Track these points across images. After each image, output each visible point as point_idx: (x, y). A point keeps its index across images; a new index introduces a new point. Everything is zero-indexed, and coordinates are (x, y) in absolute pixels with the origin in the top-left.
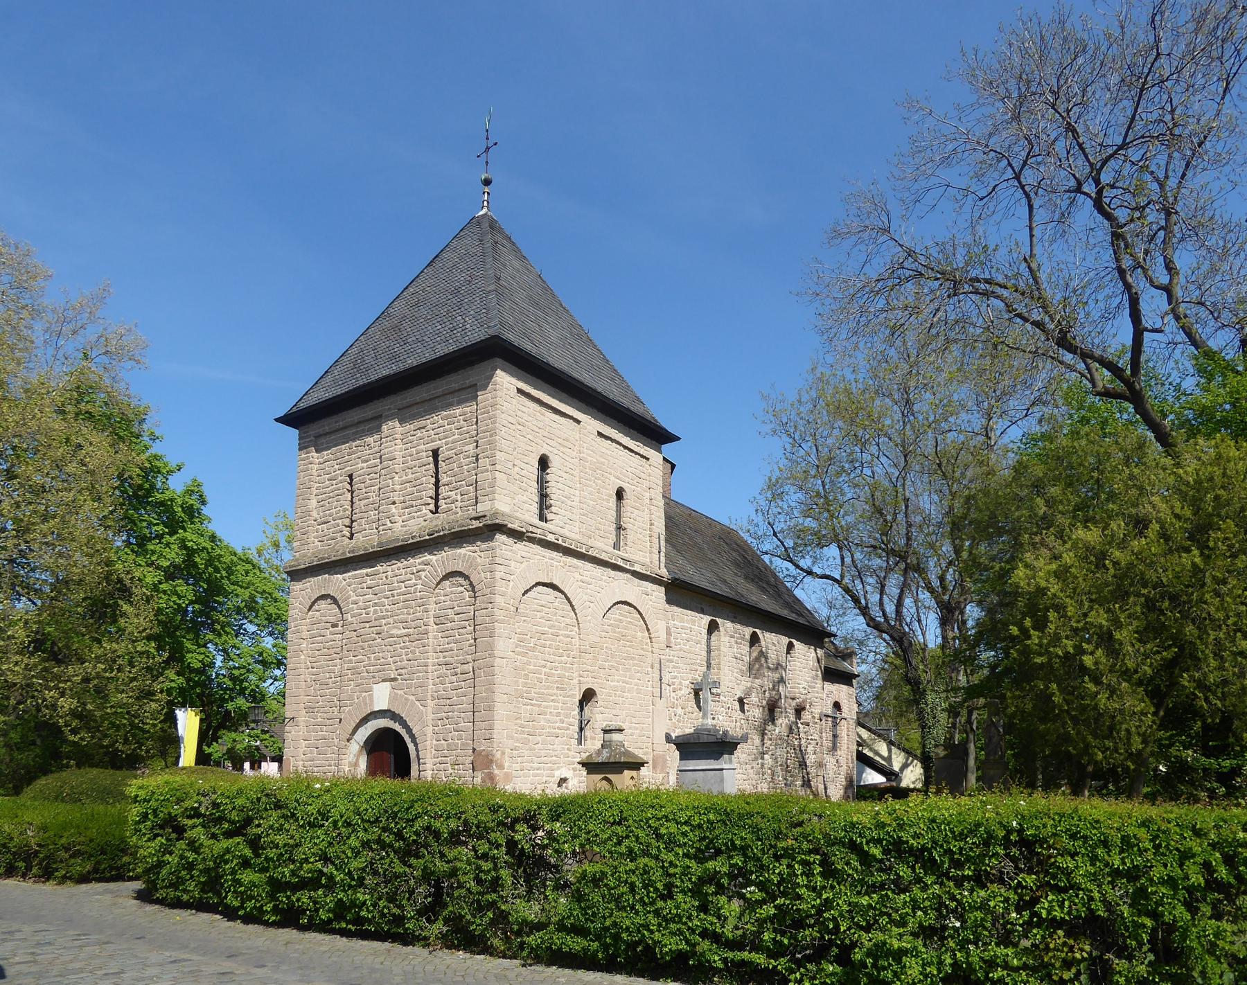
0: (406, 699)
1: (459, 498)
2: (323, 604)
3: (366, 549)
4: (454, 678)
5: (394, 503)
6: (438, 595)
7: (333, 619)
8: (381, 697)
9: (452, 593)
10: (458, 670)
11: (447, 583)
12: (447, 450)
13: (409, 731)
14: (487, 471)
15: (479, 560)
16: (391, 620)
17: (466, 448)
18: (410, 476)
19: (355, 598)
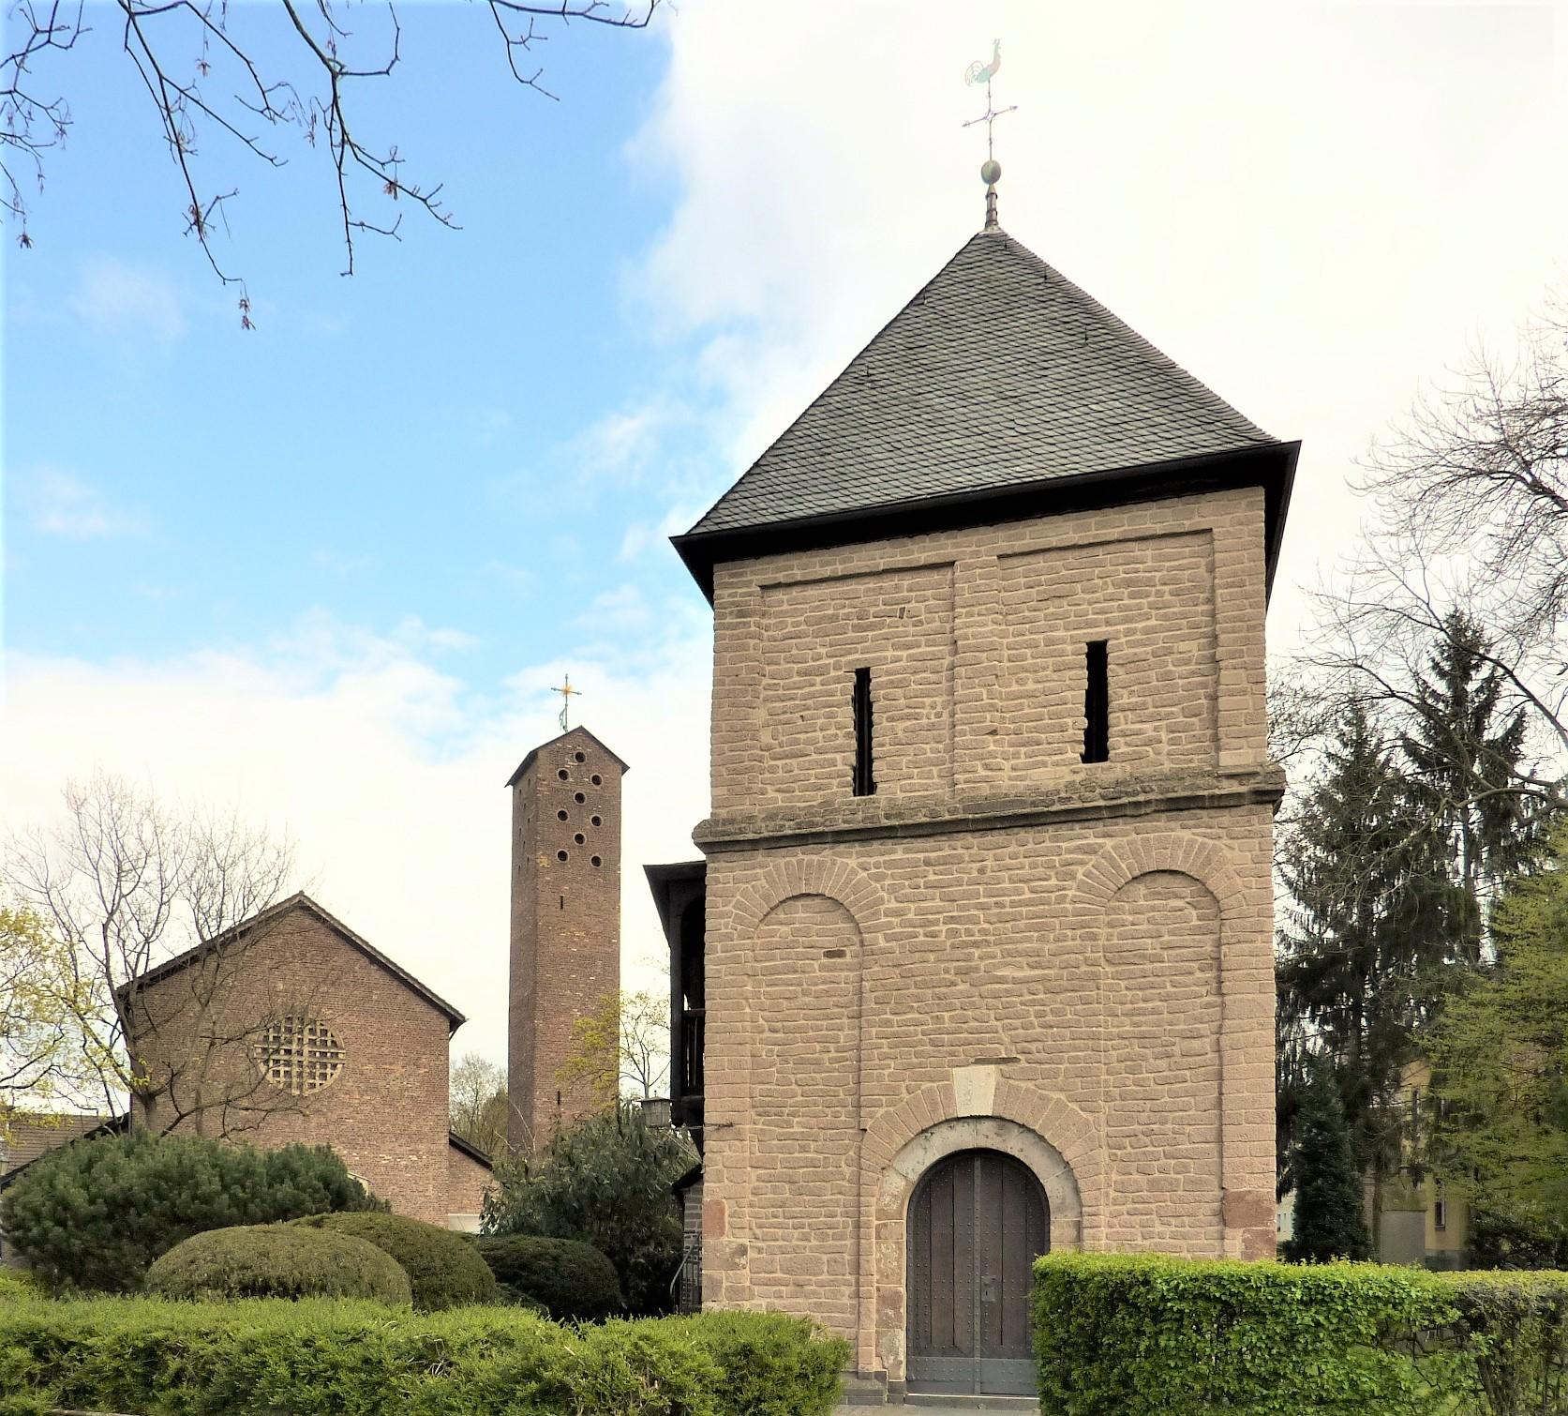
0: (1041, 1098)
1: (1164, 736)
2: (801, 912)
3: (933, 813)
4: (1163, 1063)
5: (994, 732)
6: (1115, 910)
7: (830, 943)
8: (976, 1090)
9: (1153, 909)
10: (1176, 1049)
11: (1141, 889)
12: (1131, 644)
13: (1055, 1154)
14: (1244, 692)
15: (1227, 852)
16: (997, 950)
17: (1183, 646)
18: (1031, 686)
19: (894, 905)
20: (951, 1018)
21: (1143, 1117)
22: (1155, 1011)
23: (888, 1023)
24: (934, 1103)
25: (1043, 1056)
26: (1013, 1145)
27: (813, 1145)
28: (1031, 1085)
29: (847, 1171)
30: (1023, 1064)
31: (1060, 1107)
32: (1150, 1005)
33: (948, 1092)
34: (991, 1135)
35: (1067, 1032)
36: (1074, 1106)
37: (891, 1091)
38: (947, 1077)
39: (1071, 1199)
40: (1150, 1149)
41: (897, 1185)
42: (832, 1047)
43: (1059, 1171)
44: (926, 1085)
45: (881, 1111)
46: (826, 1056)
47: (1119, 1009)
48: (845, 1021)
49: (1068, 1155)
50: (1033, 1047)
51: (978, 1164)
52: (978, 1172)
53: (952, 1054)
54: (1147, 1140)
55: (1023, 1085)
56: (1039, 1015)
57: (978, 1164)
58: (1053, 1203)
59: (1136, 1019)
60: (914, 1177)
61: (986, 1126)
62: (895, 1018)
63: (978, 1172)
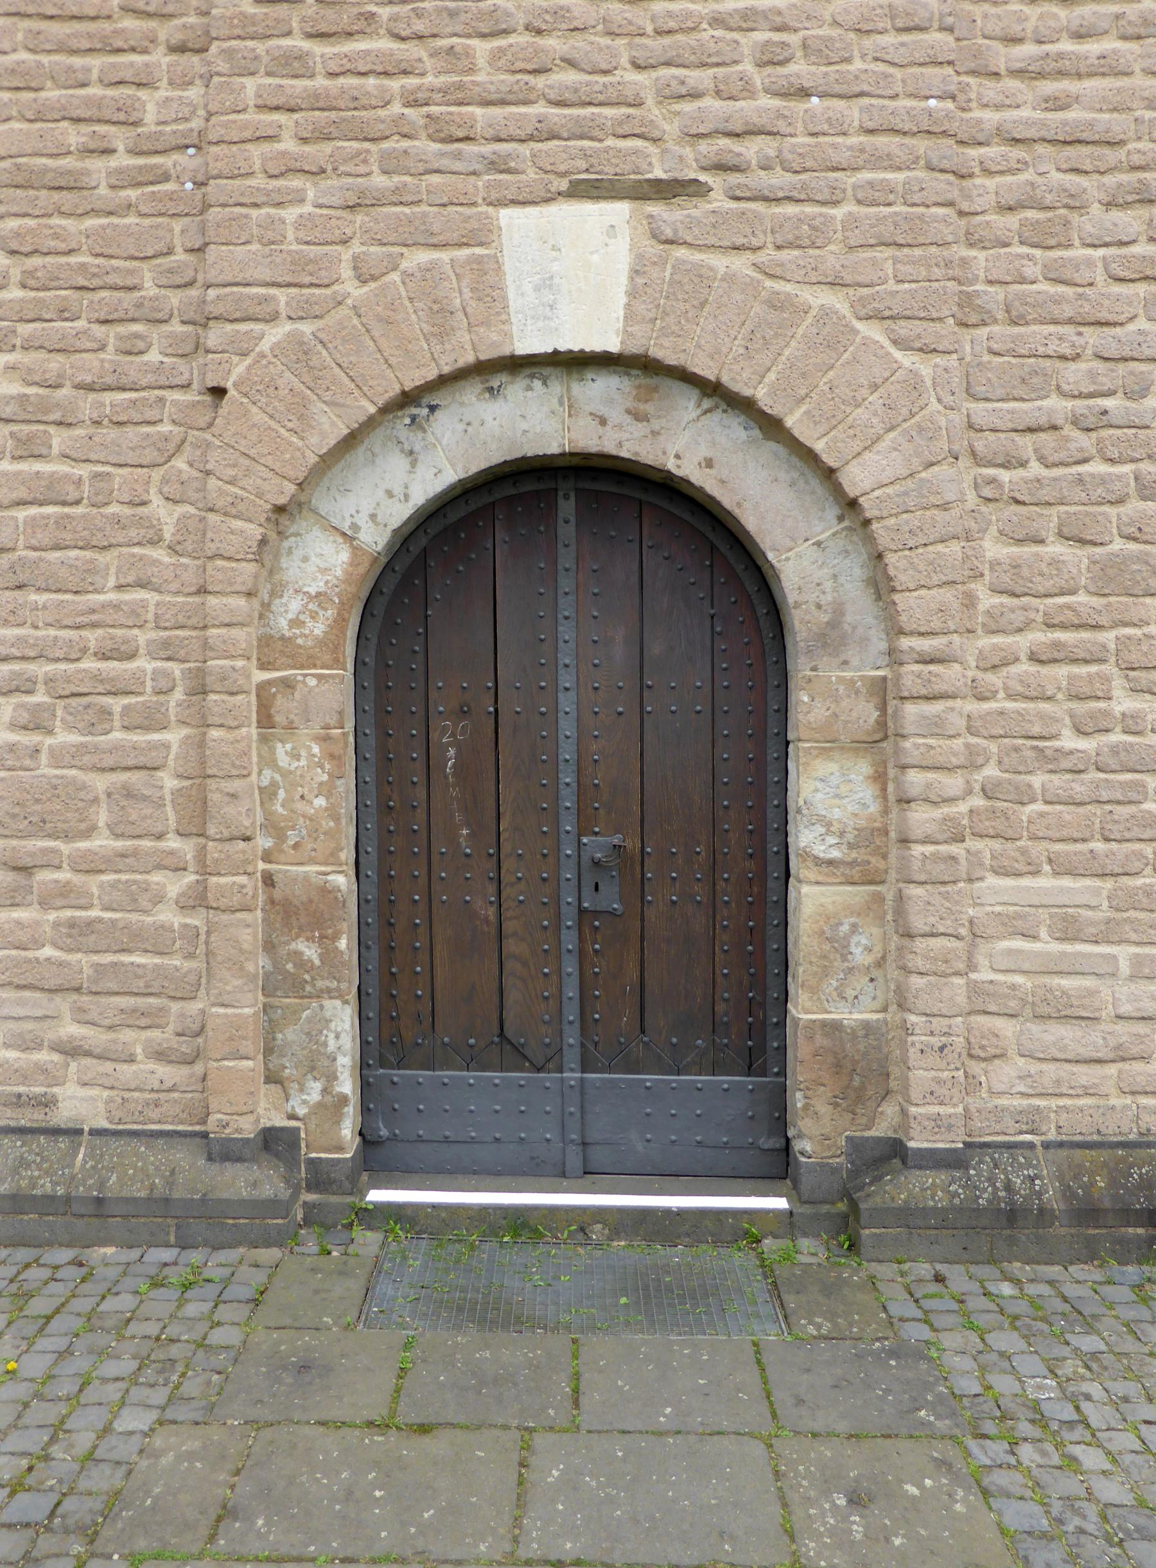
0: (777, 303)
8: (571, 276)
20: (496, 55)
21: (1074, 374)
22: (1108, 68)
23: (293, 65)
24: (440, 312)
25: (778, 180)
26: (688, 446)
27: (58, 439)
28: (740, 264)
29: (167, 516)
30: (719, 201)
31: (833, 338)
32: (1093, 48)
33: (487, 282)
34: (616, 415)
35: (853, 112)
36: (872, 331)
37: (305, 277)
38: (480, 236)
39: (861, 611)
40: (1097, 467)
41: (325, 567)
42: (120, 138)
43: (826, 523)
44: (424, 256)
45: (274, 335)
46: (97, 165)
47: (1002, 56)
48: (160, 58)
49: (857, 478)
50: (751, 150)
51: (567, 507)
52: (567, 531)
53: (496, 165)
54: (1085, 442)
55: (720, 262)
56: (769, 59)
57: (567, 507)
58: (802, 621)
59: (1049, 87)
60: (376, 539)
61: (600, 391)
62: (318, 49)
63: (567, 531)
